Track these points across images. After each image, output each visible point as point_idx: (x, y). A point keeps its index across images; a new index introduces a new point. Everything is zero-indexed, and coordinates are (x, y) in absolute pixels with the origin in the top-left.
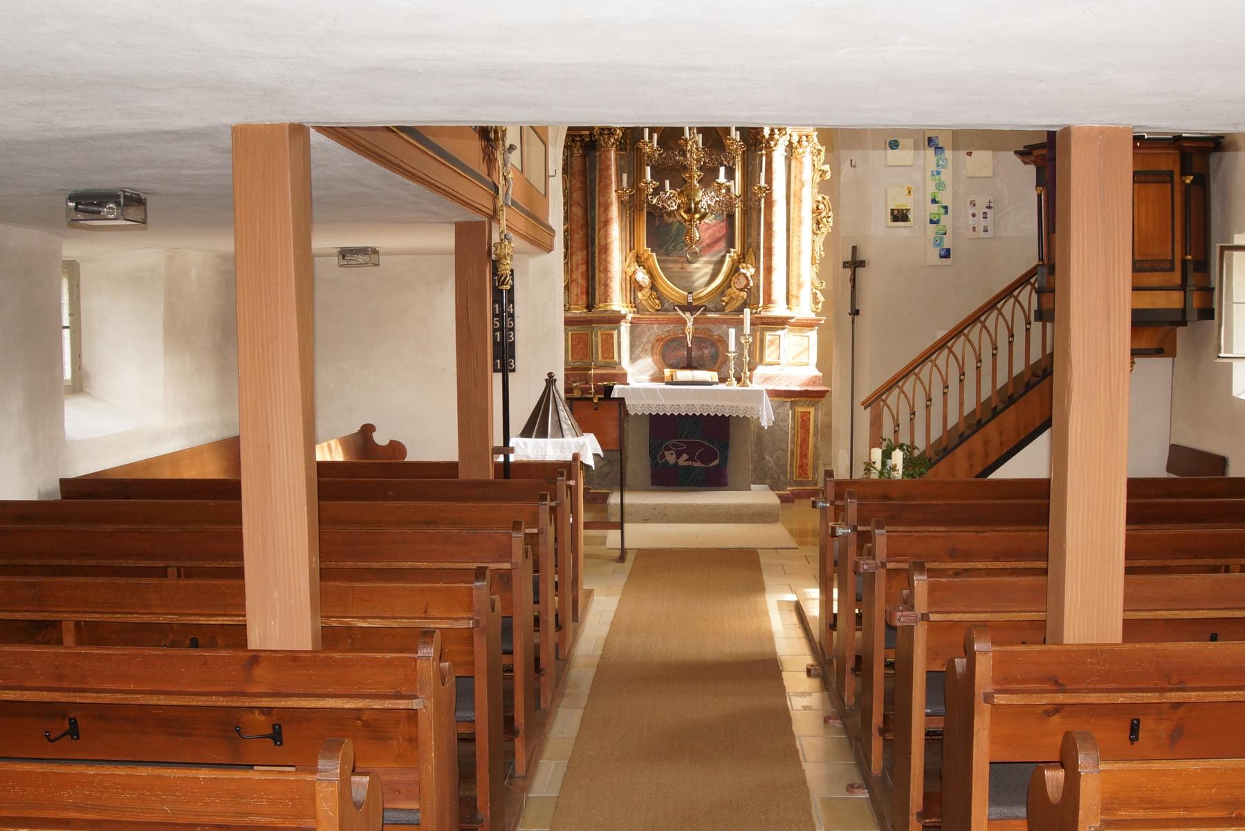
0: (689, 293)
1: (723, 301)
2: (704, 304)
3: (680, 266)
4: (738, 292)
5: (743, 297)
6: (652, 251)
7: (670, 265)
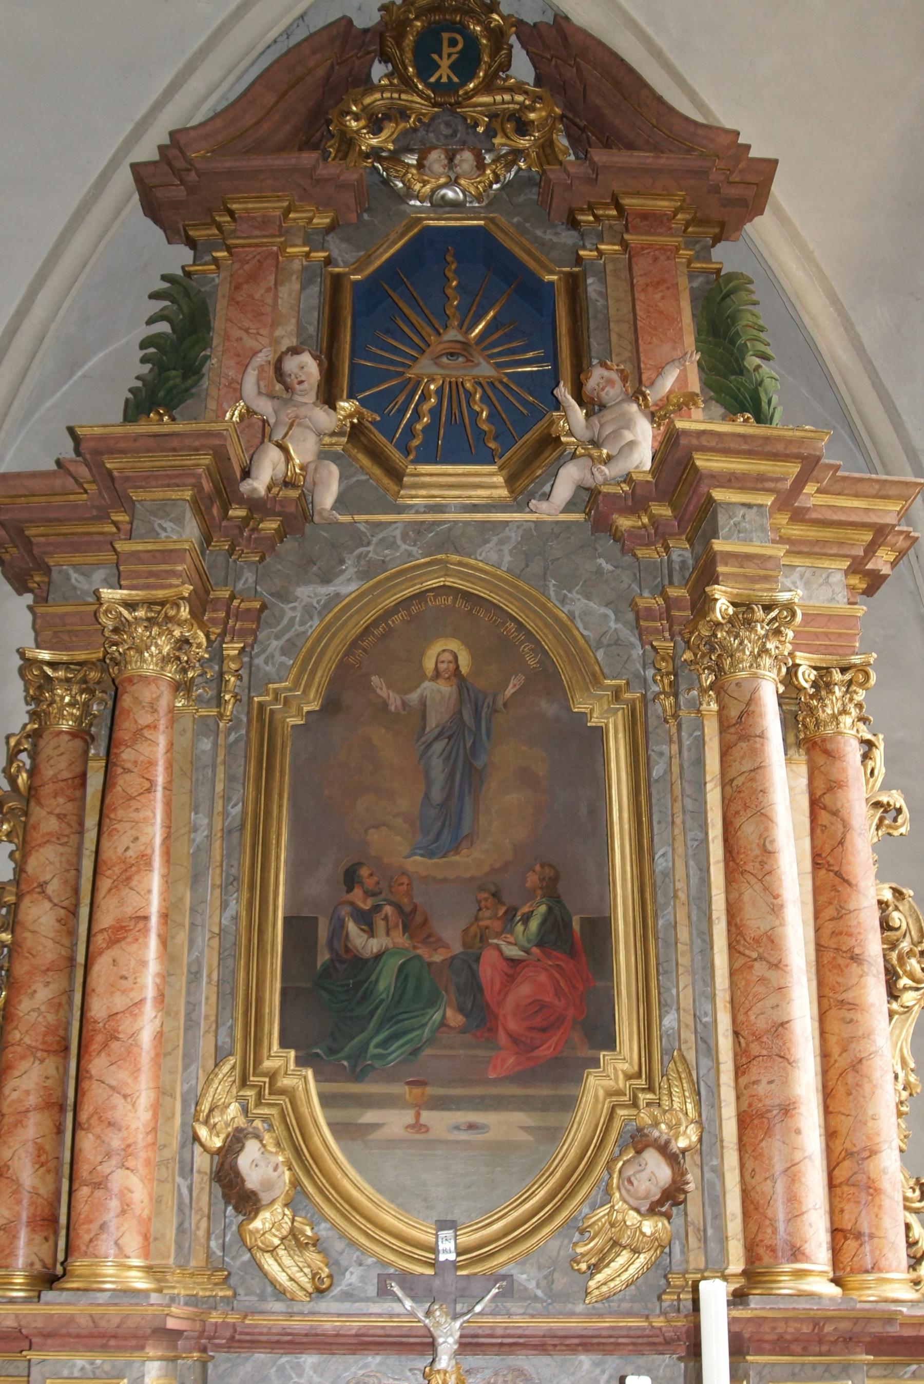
0: (442, 1225)
1: (575, 1260)
2: (503, 1271)
3: (408, 1117)
4: (633, 1218)
5: (654, 1238)
6: (300, 1062)
7: (370, 1117)
